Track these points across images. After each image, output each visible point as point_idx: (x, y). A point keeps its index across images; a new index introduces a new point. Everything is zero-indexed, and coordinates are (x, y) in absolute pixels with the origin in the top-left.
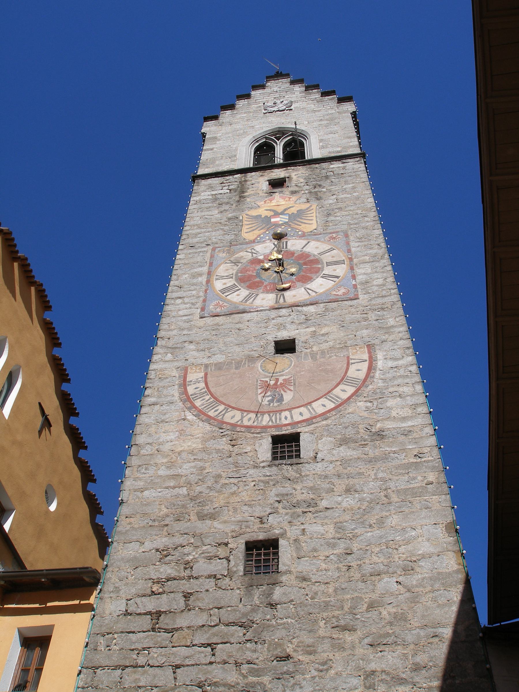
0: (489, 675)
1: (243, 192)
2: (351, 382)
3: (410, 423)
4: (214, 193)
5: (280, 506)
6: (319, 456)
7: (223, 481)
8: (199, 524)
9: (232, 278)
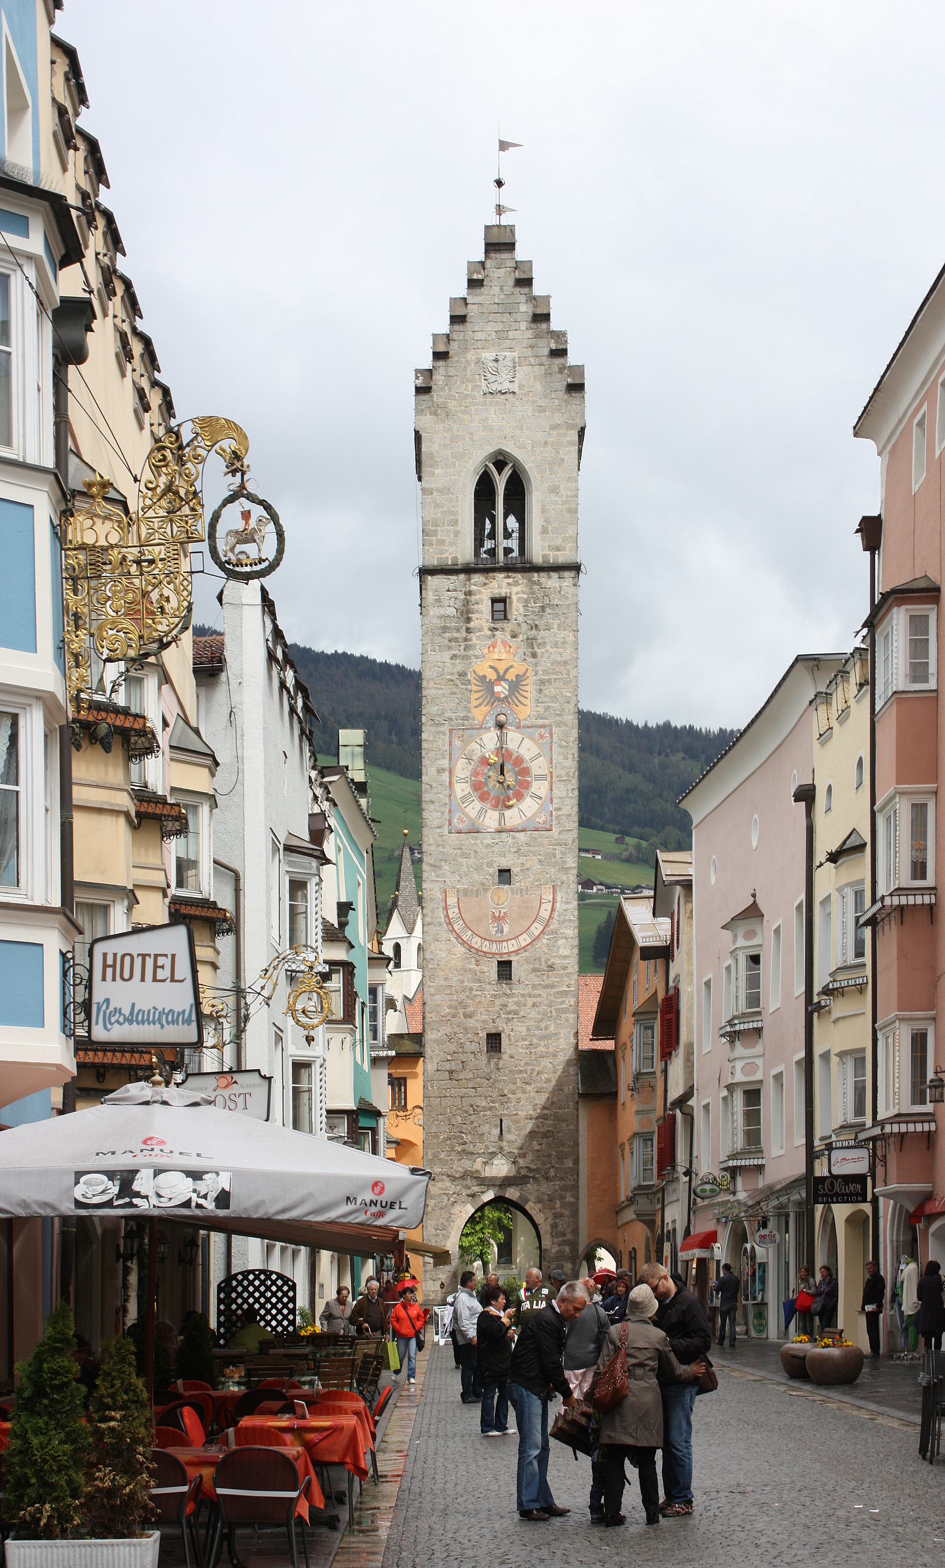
0: (577, 1110)
1: (469, 620)
4: (442, 611)
5: (502, 1012)
7: (474, 993)
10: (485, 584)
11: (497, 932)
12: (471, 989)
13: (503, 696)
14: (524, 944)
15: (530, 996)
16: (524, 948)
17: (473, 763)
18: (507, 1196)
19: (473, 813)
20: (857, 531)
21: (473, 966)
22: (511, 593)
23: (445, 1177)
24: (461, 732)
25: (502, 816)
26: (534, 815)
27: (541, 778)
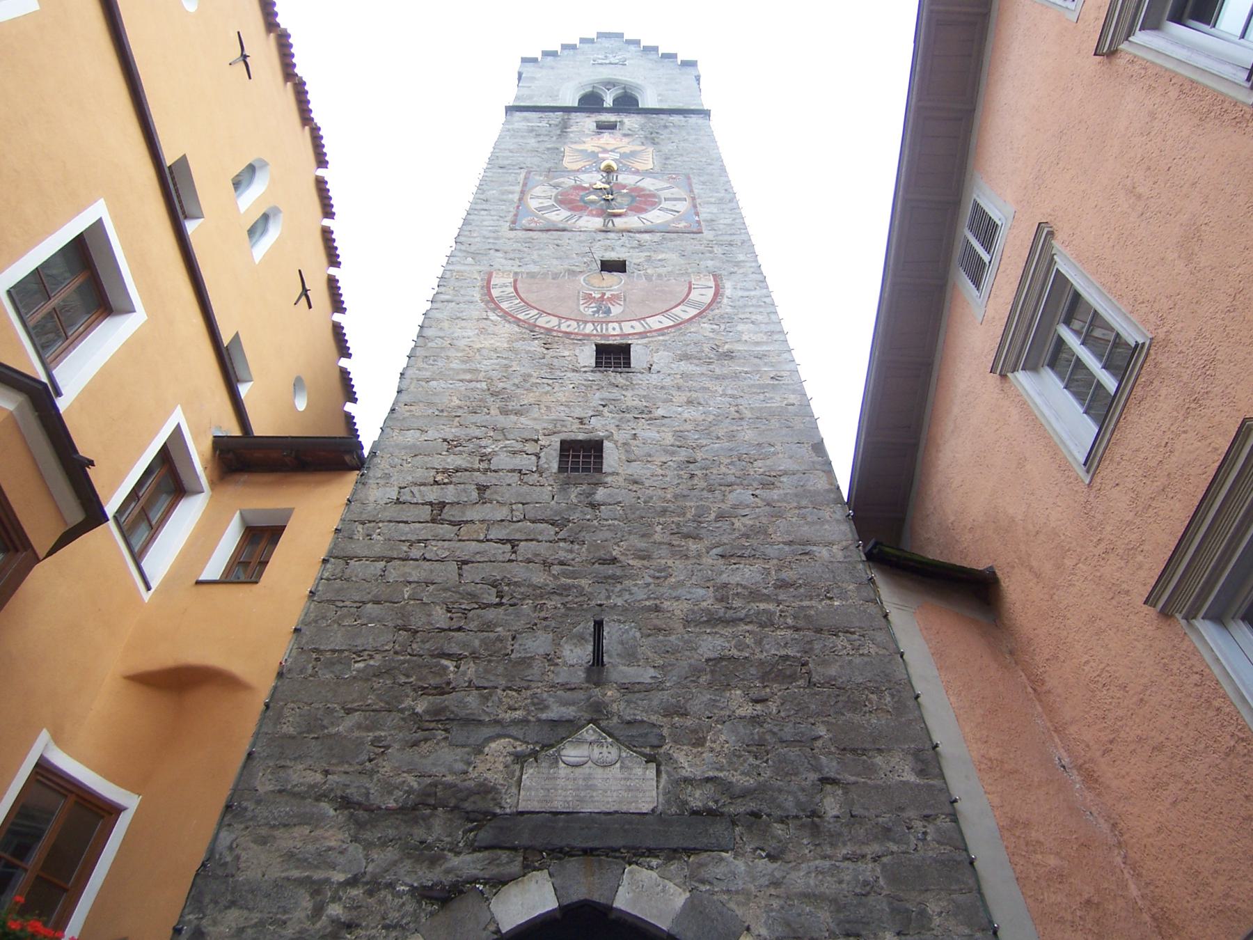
0: (876, 601)
2: (694, 304)
5: (606, 409)
8: (501, 418)
18: (623, 901)
23: (327, 808)
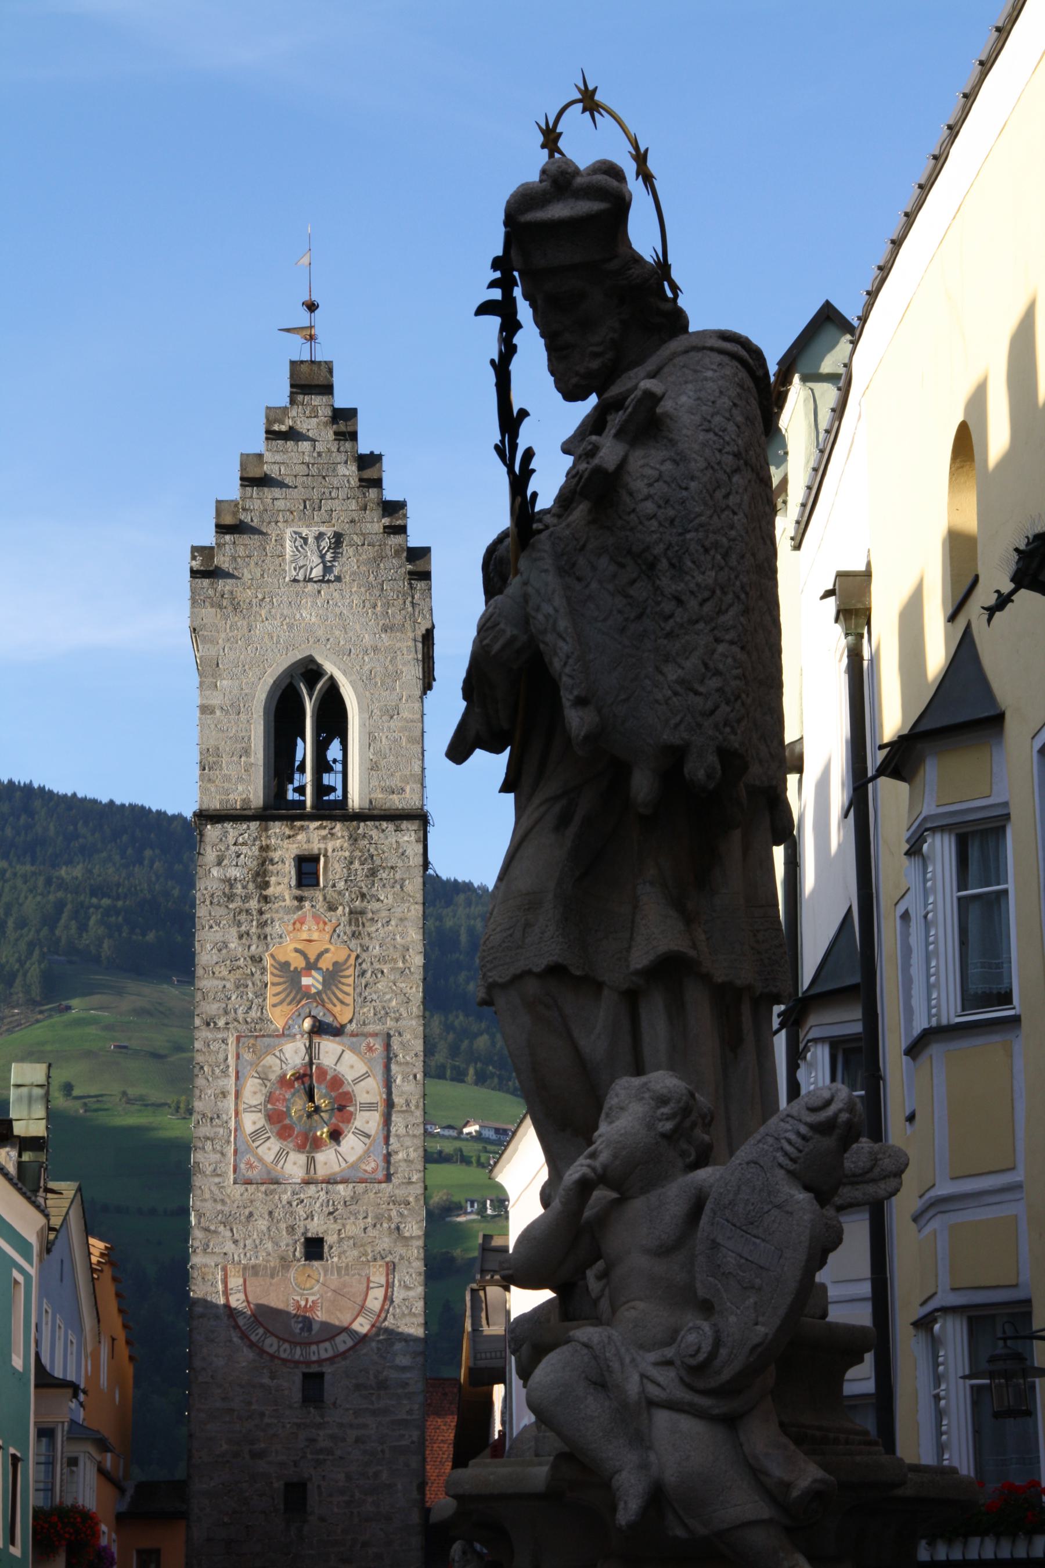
1: (267, 885)
3: (408, 1375)
6: (338, 1402)
7: (267, 1420)
9: (260, 1111)
10: (289, 837)
11: (302, 1329)
12: (262, 1415)
13: (313, 990)
14: (342, 1348)
15: (351, 1426)
16: (343, 1355)
17: (268, 1084)
19: (269, 1157)
20: (828, 594)
21: (266, 1380)
22: (326, 850)
24: (252, 1041)
25: (311, 1162)
26: (360, 1159)
27: (370, 1107)
